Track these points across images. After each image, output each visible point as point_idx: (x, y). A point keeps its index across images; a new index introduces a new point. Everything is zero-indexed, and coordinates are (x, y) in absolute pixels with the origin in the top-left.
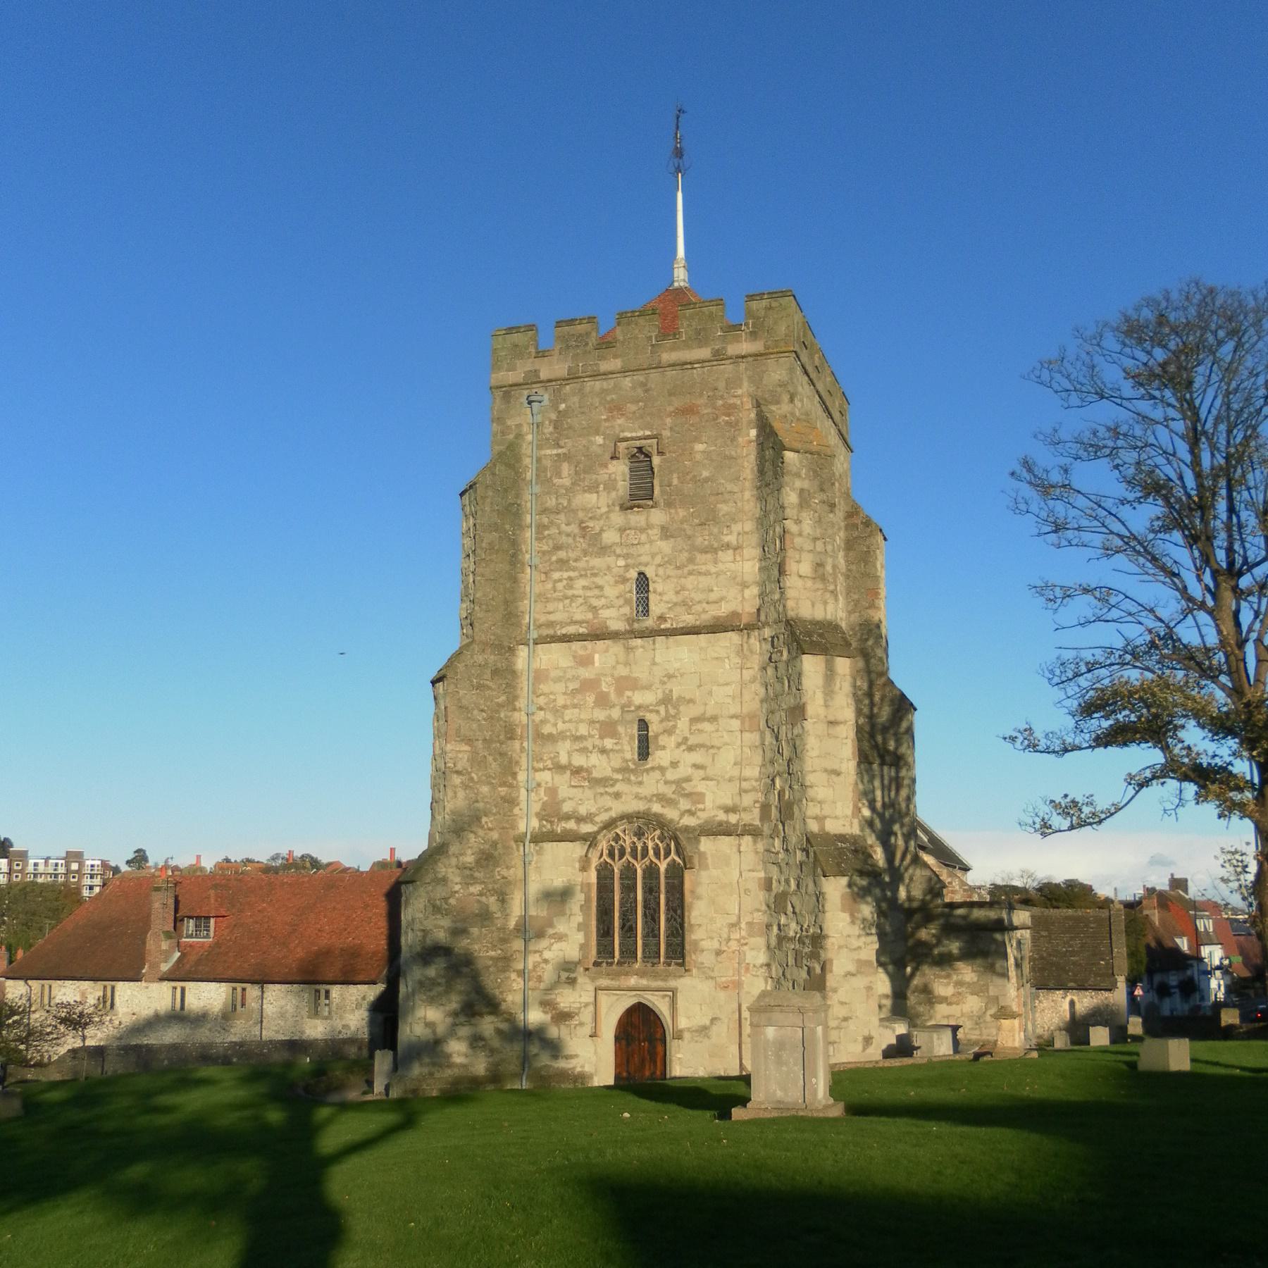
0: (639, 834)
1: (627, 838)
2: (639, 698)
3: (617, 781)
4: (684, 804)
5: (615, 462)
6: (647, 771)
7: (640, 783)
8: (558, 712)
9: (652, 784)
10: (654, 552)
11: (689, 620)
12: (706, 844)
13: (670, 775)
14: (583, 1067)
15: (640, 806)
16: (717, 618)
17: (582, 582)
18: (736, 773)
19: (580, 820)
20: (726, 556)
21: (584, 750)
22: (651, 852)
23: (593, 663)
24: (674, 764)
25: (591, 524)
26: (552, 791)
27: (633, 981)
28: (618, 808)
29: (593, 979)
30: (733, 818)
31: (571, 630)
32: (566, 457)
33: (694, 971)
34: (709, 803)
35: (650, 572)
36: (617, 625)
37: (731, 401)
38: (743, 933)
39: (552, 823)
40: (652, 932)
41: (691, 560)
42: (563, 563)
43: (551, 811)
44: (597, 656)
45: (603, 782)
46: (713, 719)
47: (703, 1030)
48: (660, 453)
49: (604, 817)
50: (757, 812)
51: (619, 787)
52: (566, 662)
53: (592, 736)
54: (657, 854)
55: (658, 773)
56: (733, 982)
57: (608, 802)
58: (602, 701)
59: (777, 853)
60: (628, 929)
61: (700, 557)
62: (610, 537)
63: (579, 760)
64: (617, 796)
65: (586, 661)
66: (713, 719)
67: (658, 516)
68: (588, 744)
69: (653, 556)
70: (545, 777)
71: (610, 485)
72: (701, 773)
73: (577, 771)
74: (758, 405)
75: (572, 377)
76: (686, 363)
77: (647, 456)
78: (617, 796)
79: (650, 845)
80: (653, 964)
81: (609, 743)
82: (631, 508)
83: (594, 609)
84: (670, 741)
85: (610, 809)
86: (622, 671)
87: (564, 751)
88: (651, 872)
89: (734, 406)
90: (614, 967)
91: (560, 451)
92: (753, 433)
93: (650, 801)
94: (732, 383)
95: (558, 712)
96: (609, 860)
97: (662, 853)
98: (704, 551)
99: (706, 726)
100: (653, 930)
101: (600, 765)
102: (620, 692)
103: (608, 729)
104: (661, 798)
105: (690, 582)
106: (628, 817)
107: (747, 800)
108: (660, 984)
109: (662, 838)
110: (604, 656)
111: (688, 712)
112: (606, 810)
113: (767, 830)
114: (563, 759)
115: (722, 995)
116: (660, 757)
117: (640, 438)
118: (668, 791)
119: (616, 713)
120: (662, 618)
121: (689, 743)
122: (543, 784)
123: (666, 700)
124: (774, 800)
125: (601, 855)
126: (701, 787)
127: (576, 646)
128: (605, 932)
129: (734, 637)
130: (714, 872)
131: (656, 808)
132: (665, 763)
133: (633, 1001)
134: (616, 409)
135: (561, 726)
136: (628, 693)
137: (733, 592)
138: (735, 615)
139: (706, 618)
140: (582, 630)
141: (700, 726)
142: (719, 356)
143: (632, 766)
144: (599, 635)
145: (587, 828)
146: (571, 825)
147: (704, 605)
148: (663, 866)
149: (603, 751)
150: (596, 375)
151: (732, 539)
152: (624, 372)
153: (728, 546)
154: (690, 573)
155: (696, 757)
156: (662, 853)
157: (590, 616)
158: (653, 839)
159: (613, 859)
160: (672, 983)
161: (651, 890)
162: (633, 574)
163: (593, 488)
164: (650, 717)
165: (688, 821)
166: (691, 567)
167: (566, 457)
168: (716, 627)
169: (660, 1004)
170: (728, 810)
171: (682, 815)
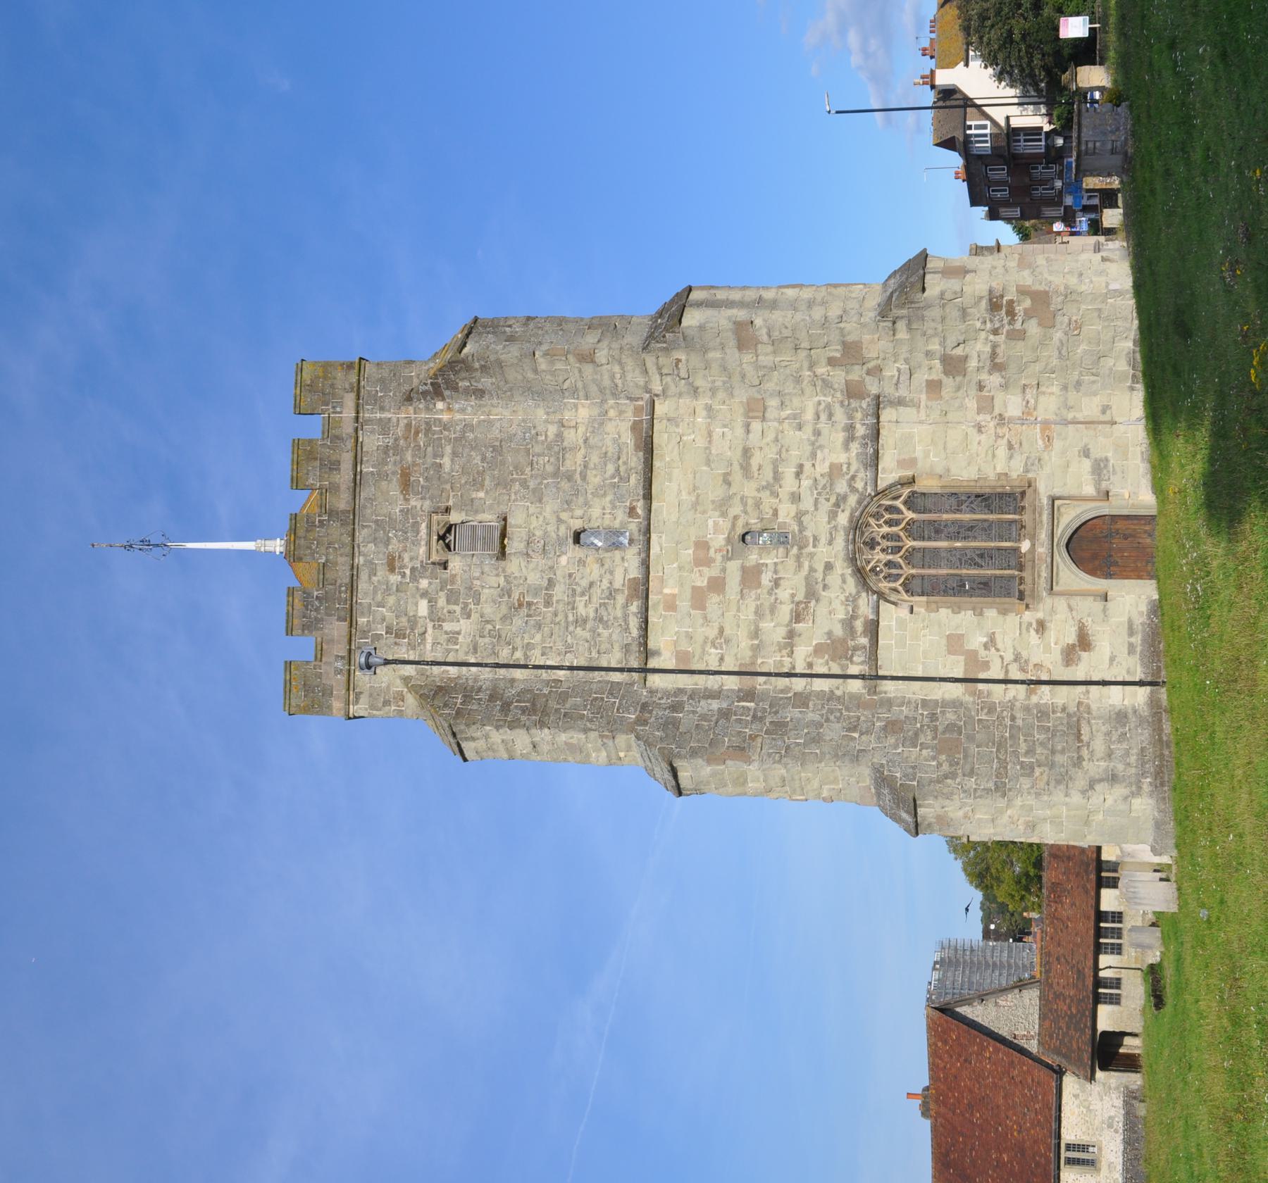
0: (872, 544)
1: (877, 557)
3: (812, 570)
5: (450, 565)
6: (802, 528)
7: (815, 539)
9: (818, 524)
11: (635, 480)
13: (807, 504)
14: (1141, 613)
16: (637, 448)
17: (581, 610)
18: (808, 429)
20: (571, 437)
21: (773, 610)
22: (895, 529)
23: (674, 596)
24: (796, 498)
25: (516, 595)
28: (842, 568)
29: (1040, 599)
30: (861, 430)
31: (634, 623)
33: (1030, 475)
34: (842, 458)
35: (577, 524)
37: (400, 432)
38: (988, 417)
39: (855, 649)
40: (987, 529)
41: (569, 478)
44: (666, 591)
46: (747, 453)
47: (1099, 468)
48: (447, 510)
49: (851, 585)
50: (854, 404)
53: (758, 598)
54: (897, 523)
55: (805, 519)
56: (1043, 431)
57: (834, 579)
58: (717, 585)
59: (899, 370)
61: (568, 465)
63: (785, 611)
64: (829, 567)
65: (671, 605)
66: (747, 453)
69: (560, 520)
72: (808, 466)
73: (797, 617)
74: (409, 399)
76: (355, 479)
77: (449, 530)
78: (829, 567)
79: (886, 529)
80: (1023, 527)
81: (766, 579)
82: (503, 547)
83: (612, 593)
84: (768, 502)
85: (842, 575)
87: (774, 631)
89: (409, 426)
90: (1024, 574)
91: (430, 630)
92: (440, 405)
93: (835, 527)
94: (384, 426)
96: (901, 580)
97: (895, 516)
99: (755, 462)
100: (984, 529)
102: (708, 562)
103: (750, 577)
104: (833, 515)
105: (594, 479)
108: (1045, 517)
109: (877, 516)
112: (844, 581)
114: (782, 631)
115: (1057, 444)
117: (429, 535)
118: (825, 506)
119: (734, 567)
120: (632, 512)
121: (771, 481)
122: (809, 660)
124: (839, 377)
125: (895, 590)
126: (822, 468)
128: (985, 588)
130: (919, 453)
131: (843, 519)
132: (793, 509)
133: (1063, 550)
136: (712, 551)
138: (635, 427)
139: (635, 460)
140: (634, 607)
141: (755, 468)
143: (795, 550)
144: (642, 589)
146: (859, 625)
147: (620, 462)
148: (910, 515)
149: (777, 583)
150: (352, 587)
151: (552, 430)
153: (559, 436)
154: (584, 477)
155: (789, 471)
156: (895, 516)
157: (621, 599)
158: (879, 526)
159: (899, 576)
160: (1045, 501)
161: (937, 530)
166: (577, 477)
168: (648, 448)
169: (1069, 518)
170: (850, 438)
171: (853, 489)
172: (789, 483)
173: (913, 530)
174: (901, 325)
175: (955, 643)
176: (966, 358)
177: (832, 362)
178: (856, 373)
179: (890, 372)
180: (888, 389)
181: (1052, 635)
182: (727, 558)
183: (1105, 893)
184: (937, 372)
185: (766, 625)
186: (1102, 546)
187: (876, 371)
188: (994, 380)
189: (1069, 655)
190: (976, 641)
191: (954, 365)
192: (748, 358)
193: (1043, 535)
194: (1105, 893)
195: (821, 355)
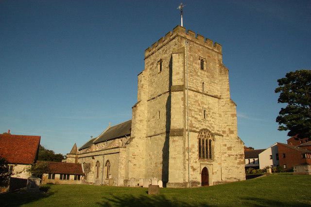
2: (206, 107)
4: (212, 128)
8: (192, 105)
10: (206, 80)
11: (211, 94)
12: (216, 137)
15: (205, 127)
19: (197, 128)
26: (191, 121)
27: (206, 162)
30: (219, 132)
31: (194, 89)
32: (191, 55)
36: (201, 91)
42: (192, 76)
43: (191, 125)
45: (199, 121)
51: (202, 123)
52: (193, 96)
60: (203, 152)
62: (199, 74)
63: (196, 116)
65: (196, 96)
67: (206, 73)
68: (197, 113)
70: (190, 118)
71: (199, 64)
73: (196, 118)
75: (192, 41)
78: (202, 125)
79: (207, 135)
81: (200, 114)
86: (202, 100)
88: (207, 141)
95: (192, 105)
98: (213, 82)
101: (200, 118)
103: (200, 111)
105: (211, 87)
106: (205, 129)
107: (220, 130)
110: (200, 96)
111: (212, 111)
113: (225, 135)
116: (208, 119)
118: (209, 125)
123: (208, 108)
124: (227, 130)
127: (195, 93)
129: (217, 99)
131: (208, 128)
134: (199, 51)
135: (192, 108)
137: (217, 92)
139: (213, 95)
142: (213, 50)
145: (198, 130)
146: (195, 129)
152: (201, 45)
162: (202, 82)
163: (196, 63)
164: (207, 110)
165: (213, 132)
167: (191, 55)
170: (218, 131)
172: (212, 120)
173: (207, 141)
174: (237, 140)
175: (193, 146)
176: (231, 150)
177: (229, 129)
178: (228, 132)
179: (227, 138)
180: (224, 138)
181: (195, 164)
182: (203, 107)
183: (59, 175)
184: (228, 146)
185: (193, 113)
186: (205, 173)
187: (228, 136)
188: (226, 155)
189: (192, 167)
190: (193, 150)
191: (229, 148)
192: (230, 116)
193: (208, 163)
194: (59, 175)
195: (230, 127)
